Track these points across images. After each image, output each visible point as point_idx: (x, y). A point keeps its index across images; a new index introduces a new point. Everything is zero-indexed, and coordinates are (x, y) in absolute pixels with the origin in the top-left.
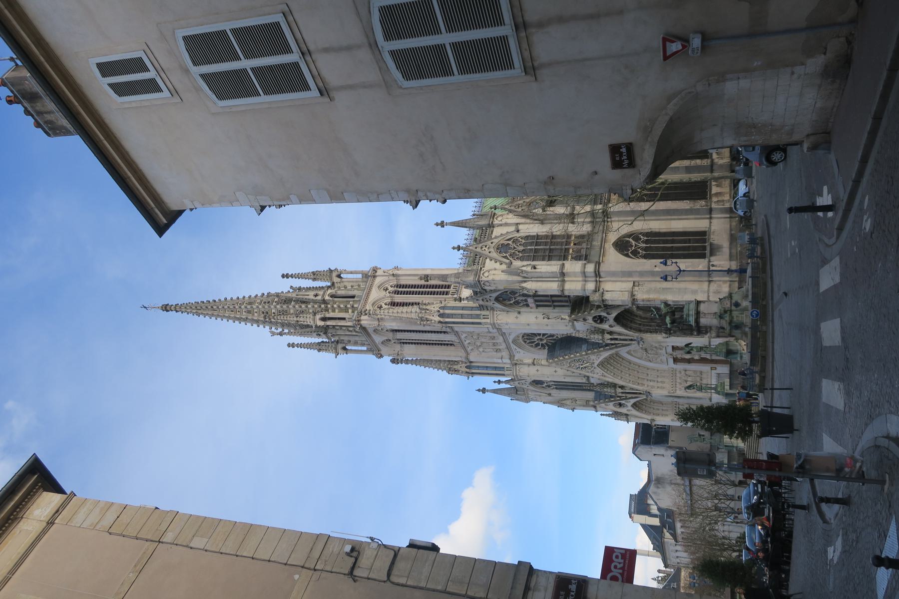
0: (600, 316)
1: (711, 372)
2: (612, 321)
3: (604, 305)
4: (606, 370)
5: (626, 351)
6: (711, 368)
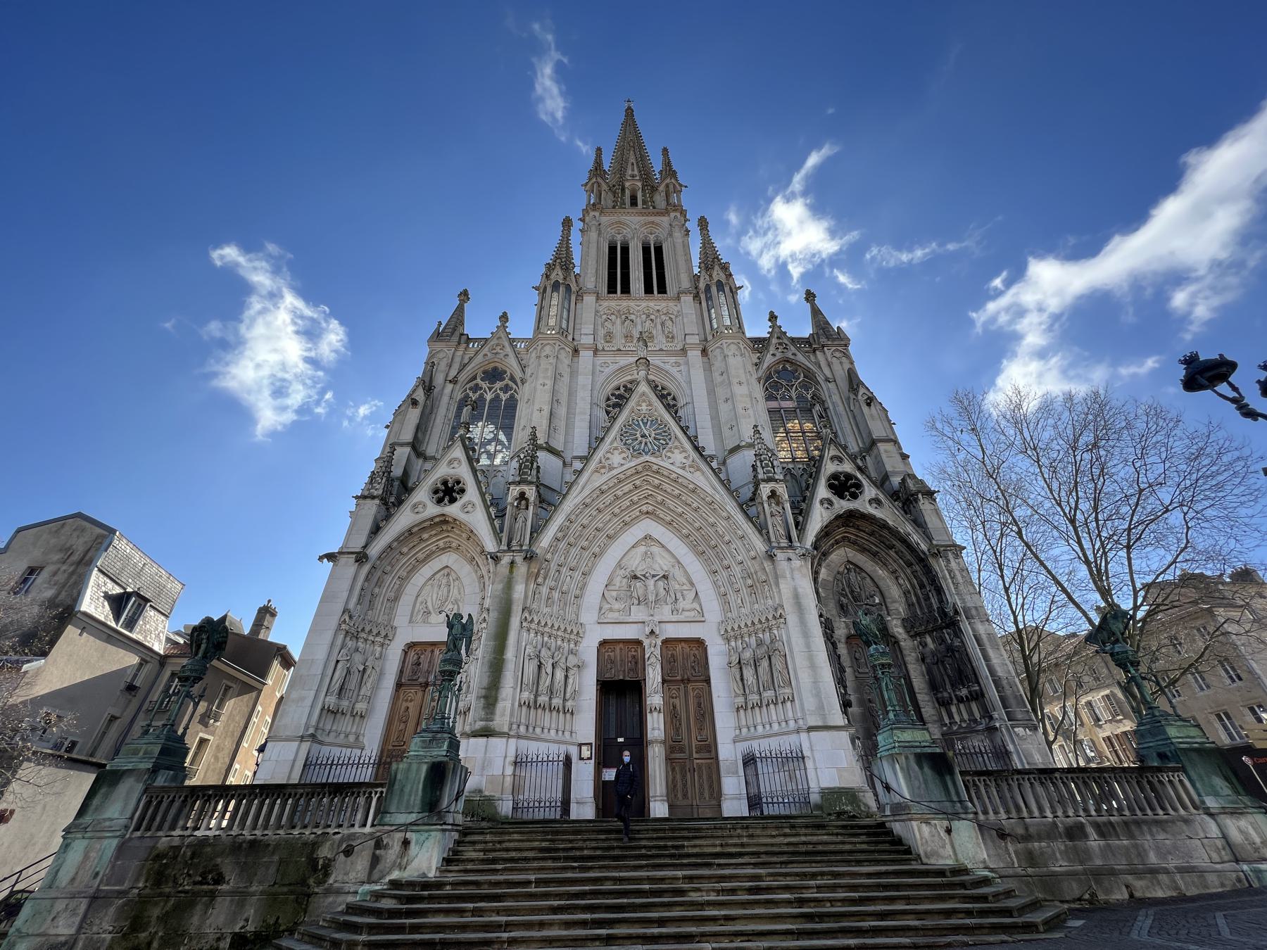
0: (859, 486)
1: (573, 744)
2: (843, 505)
5: (655, 536)
6: (591, 744)
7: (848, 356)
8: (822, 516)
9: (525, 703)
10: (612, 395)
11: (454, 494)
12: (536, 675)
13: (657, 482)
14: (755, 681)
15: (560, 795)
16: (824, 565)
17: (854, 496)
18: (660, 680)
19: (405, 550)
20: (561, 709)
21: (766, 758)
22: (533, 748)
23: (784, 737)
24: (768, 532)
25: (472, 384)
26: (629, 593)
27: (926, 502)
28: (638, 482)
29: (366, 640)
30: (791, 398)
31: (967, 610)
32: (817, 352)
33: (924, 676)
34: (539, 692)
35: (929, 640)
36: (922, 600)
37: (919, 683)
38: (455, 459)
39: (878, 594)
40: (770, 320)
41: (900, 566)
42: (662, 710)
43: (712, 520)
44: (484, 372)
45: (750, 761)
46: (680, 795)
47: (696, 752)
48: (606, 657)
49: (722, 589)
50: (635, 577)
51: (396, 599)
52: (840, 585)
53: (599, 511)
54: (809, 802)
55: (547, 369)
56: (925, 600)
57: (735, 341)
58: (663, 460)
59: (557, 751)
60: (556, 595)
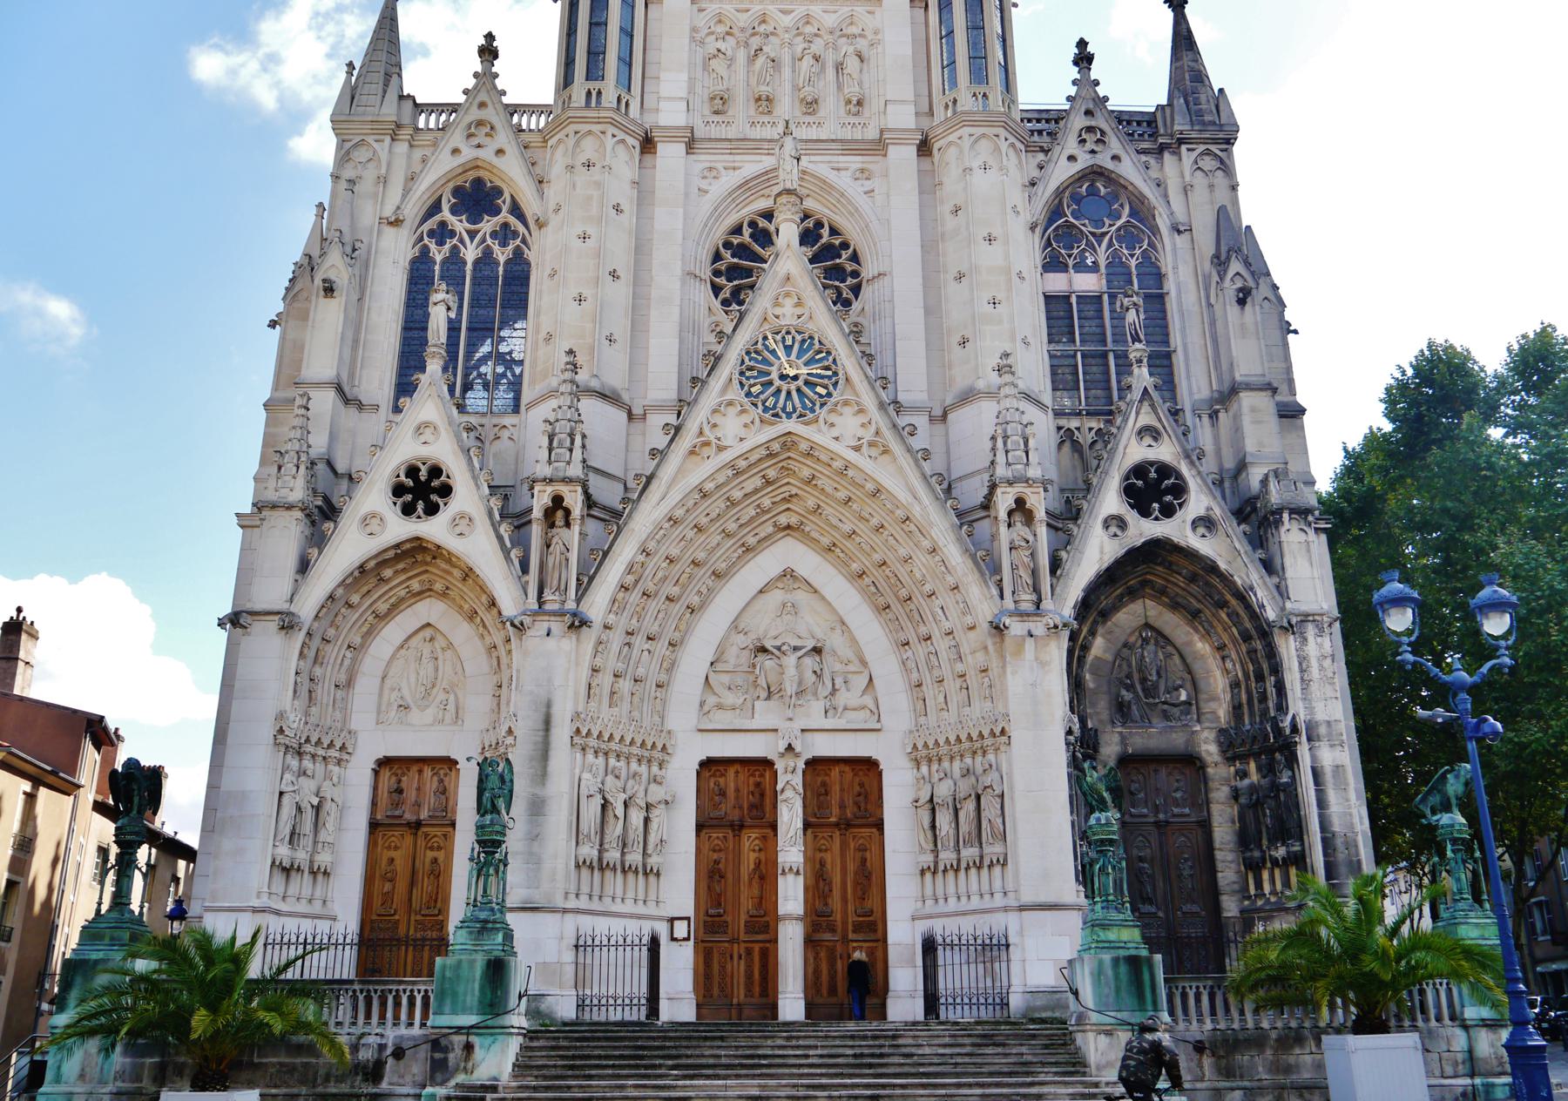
0: (1180, 490)
1: (660, 918)
2: (1144, 529)
3: (1279, 511)
4: (742, 464)
5: (802, 570)
6: (688, 919)
7: (1226, 167)
8: (1102, 552)
9: (584, 862)
10: (727, 245)
11: (434, 497)
12: (598, 821)
13: (806, 473)
14: (952, 832)
15: (644, 989)
16: (1100, 630)
17: (1168, 512)
18: (800, 825)
19: (355, 599)
20: (640, 869)
21: (952, 945)
22: (602, 927)
23: (986, 916)
24: (1001, 580)
25: (431, 223)
26: (752, 678)
27: (1295, 526)
28: (772, 473)
29: (313, 756)
30: (1095, 268)
31: (1311, 728)
32: (1167, 155)
33: (1233, 822)
34: (606, 846)
35: (1252, 766)
36: (1256, 701)
37: (1223, 832)
38: (426, 425)
39: (1189, 685)
40: (1076, 63)
41: (1232, 636)
42: (801, 871)
43: (902, 552)
44: (457, 191)
45: (929, 947)
46: (825, 991)
47: (854, 932)
48: (712, 785)
49: (915, 675)
50: (763, 650)
51: (350, 683)
52: (1125, 666)
53: (699, 529)
54: (1008, 1004)
55: (589, 198)
56: (1260, 702)
57: (990, 131)
58: (820, 431)
59: (638, 930)
60: (625, 685)
